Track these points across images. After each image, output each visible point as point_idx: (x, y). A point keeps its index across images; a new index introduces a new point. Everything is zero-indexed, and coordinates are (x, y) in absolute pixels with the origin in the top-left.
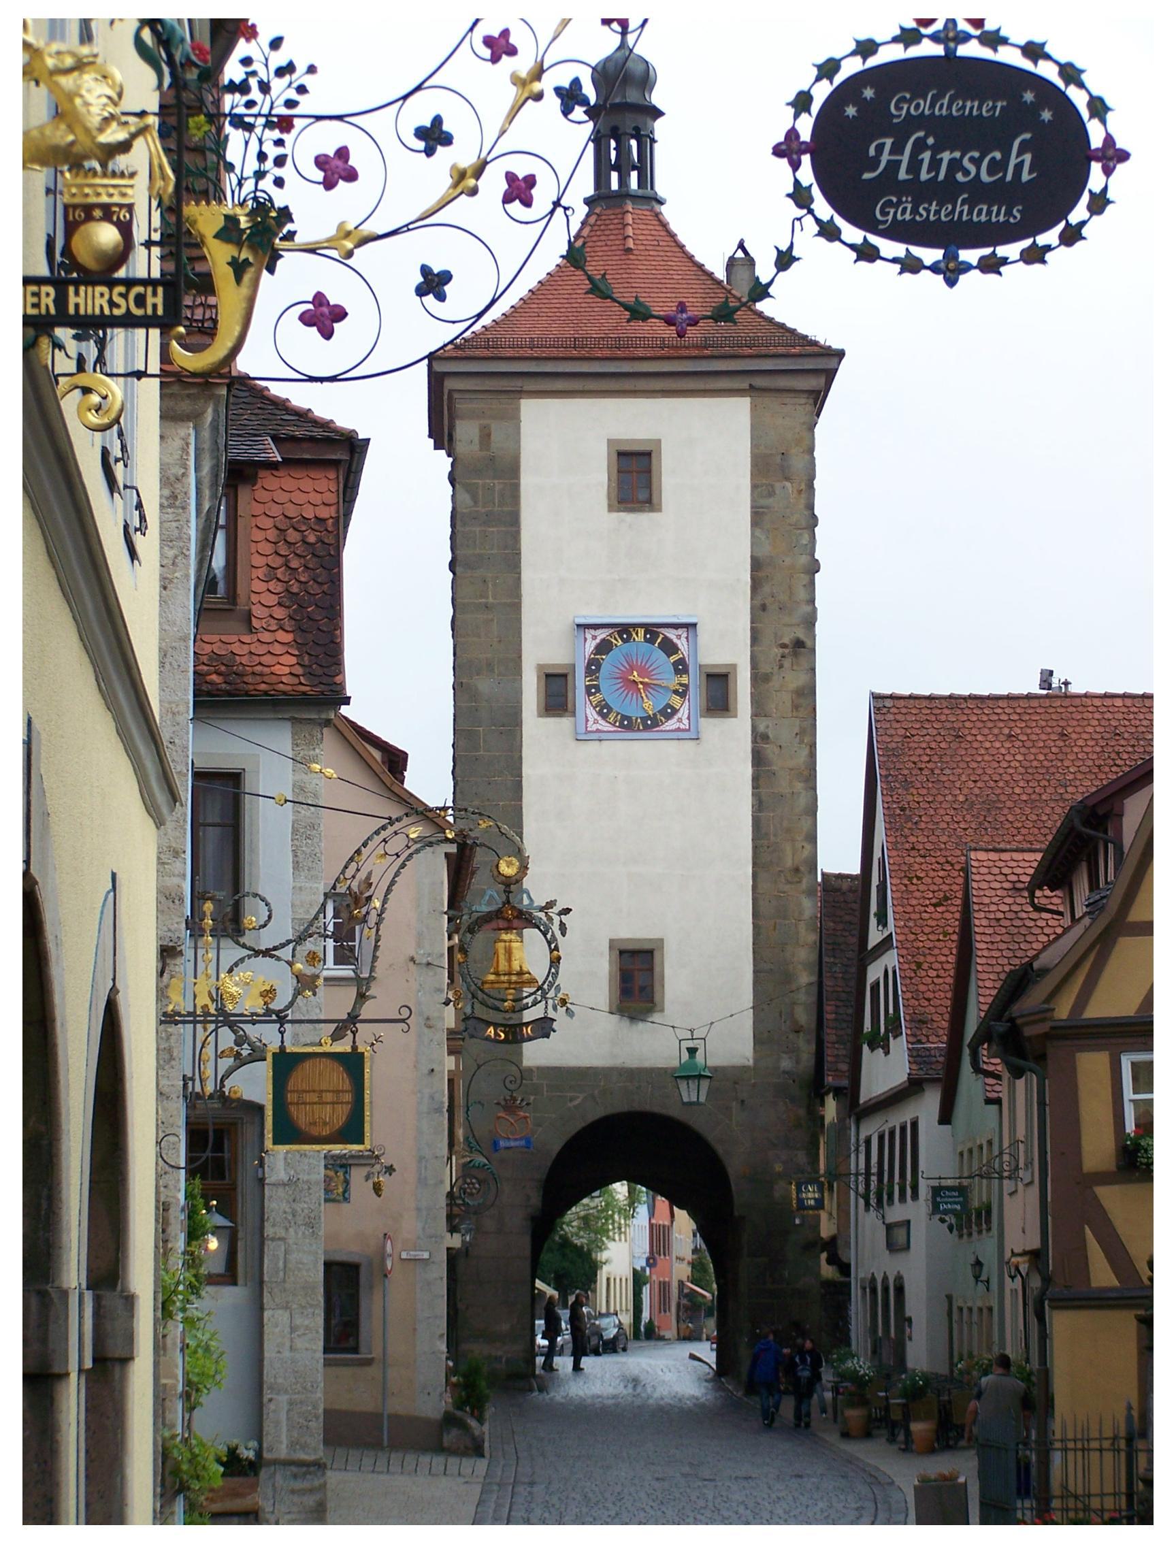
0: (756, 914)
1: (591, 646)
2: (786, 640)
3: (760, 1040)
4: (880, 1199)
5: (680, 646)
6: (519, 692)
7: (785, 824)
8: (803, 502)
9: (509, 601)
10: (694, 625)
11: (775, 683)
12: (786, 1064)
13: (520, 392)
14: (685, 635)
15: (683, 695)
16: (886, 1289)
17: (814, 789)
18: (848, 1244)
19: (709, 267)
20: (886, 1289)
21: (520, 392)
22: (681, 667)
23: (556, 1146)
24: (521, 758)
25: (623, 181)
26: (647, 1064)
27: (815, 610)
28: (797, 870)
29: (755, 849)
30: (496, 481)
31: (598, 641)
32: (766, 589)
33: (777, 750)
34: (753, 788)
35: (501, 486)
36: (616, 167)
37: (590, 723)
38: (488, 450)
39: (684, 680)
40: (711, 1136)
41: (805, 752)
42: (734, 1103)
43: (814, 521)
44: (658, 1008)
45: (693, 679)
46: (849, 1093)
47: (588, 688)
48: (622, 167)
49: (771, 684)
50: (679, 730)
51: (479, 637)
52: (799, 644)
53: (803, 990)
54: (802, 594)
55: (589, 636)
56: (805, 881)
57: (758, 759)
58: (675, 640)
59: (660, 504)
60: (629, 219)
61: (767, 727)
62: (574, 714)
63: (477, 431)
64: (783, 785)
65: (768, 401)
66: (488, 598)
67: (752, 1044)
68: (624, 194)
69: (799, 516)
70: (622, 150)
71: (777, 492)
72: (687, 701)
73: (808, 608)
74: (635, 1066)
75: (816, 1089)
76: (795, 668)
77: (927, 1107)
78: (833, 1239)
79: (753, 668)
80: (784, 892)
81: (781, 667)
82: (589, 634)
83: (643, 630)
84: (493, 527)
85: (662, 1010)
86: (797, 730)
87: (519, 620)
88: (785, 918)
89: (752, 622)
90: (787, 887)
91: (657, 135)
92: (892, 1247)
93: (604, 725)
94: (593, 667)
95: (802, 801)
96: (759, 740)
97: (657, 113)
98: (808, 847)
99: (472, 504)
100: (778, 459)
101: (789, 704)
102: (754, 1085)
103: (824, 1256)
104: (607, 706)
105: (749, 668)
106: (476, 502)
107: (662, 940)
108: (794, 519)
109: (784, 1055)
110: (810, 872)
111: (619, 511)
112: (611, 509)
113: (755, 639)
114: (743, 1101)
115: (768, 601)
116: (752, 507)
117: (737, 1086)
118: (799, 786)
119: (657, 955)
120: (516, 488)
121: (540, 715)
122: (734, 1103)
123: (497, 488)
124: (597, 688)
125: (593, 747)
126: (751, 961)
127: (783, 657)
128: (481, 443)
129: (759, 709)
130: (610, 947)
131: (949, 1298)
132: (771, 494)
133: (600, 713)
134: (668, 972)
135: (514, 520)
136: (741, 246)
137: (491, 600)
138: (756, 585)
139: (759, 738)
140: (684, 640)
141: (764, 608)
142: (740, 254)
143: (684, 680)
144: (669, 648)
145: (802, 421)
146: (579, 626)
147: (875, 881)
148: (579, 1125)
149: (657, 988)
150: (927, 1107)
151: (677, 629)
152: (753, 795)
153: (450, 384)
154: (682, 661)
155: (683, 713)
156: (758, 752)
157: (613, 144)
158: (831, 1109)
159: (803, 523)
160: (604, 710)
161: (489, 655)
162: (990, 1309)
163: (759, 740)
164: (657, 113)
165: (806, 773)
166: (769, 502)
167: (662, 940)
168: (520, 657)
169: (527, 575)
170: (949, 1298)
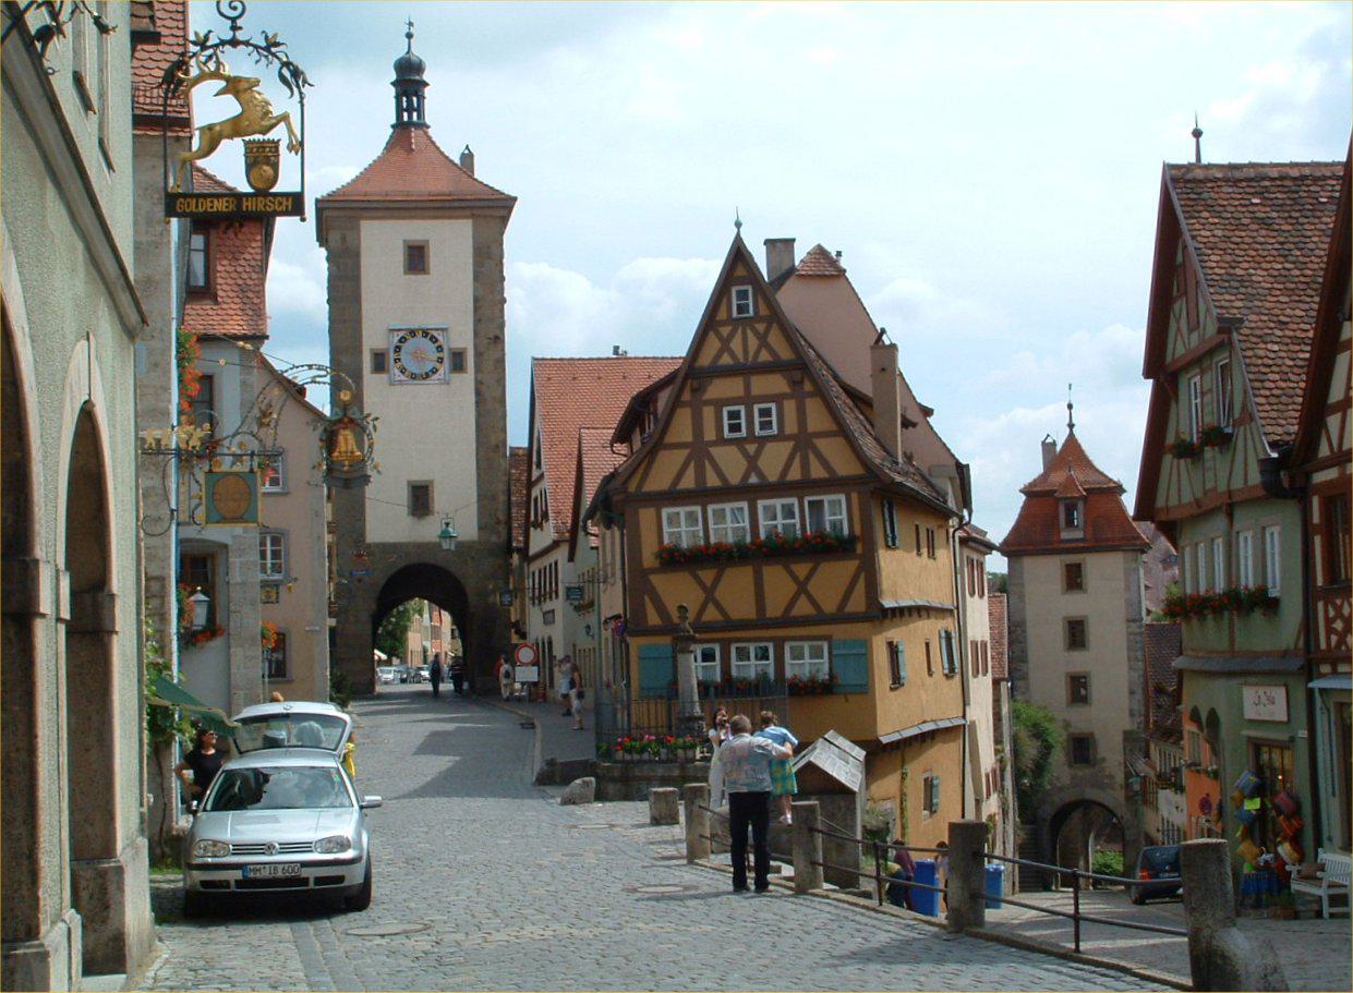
1: (396, 339)
2: (491, 336)
3: (480, 528)
4: (540, 598)
6: (361, 362)
10: (446, 329)
12: (494, 539)
16: (543, 644)
17: (505, 406)
18: (524, 623)
19: (452, 157)
20: (543, 644)
22: (440, 349)
23: (383, 582)
25: (410, 116)
26: (426, 540)
28: (497, 446)
29: (478, 436)
36: (406, 110)
39: (441, 355)
41: (500, 388)
43: (503, 279)
45: (445, 355)
46: (524, 551)
48: (410, 110)
57: (478, 393)
60: (413, 134)
68: (410, 123)
70: (410, 102)
75: (508, 550)
77: (561, 554)
78: (517, 622)
82: (395, 333)
91: (426, 95)
92: (546, 623)
93: (403, 378)
94: (398, 349)
97: (426, 84)
103: (513, 630)
112: (405, 273)
113: (476, 334)
119: (430, 488)
125: (398, 388)
127: (489, 344)
129: (478, 369)
131: (574, 646)
134: (435, 495)
136: (467, 147)
138: (476, 309)
139: (478, 383)
141: (480, 320)
142: (467, 152)
143: (441, 355)
144: (434, 340)
147: (535, 448)
148: (395, 570)
149: (430, 500)
150: (561, 554)
153: (326, 213)
154: (440, 346)
155: (441, 371)
157: (405, 99)
158: (516, 558)
160: (403, 370)
162: (594, 649)
164: (426, 84)
166: (482, 269)
169: (365, 306)
170: (574, 646)
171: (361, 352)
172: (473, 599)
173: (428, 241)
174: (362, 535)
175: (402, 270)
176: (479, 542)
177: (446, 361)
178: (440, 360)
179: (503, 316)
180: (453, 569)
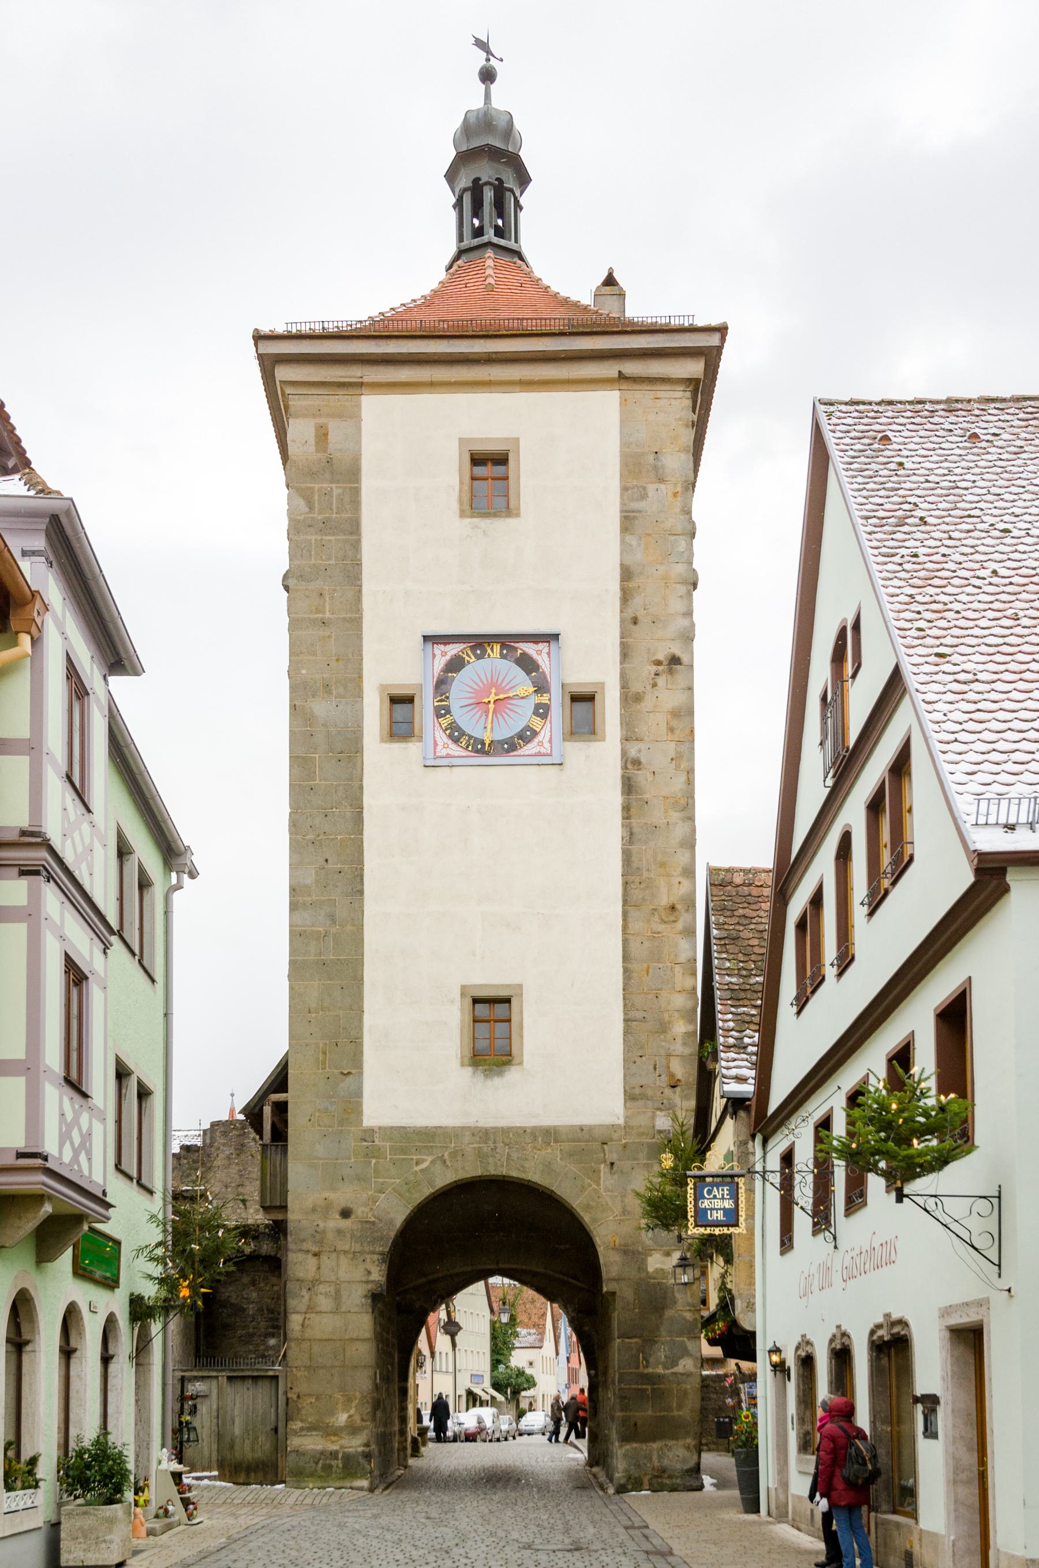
0: (626, 958)
1: (440, 663)
2: (661, 657)
3: (630, 1097)
5: (540, 662)
7: (660, 858)
8: (678, 503)
9: (349, 615)
10: (556, 637)
11: (648, 704)
12: (663, 1122)
13: (361, 385)
14: (546, 650)
15: (544, 716)
17: (691, 818)
21: (361, 385)
24: (361, 788)
27: (693, 625)
29: (626, 884)
30: (334, 486)
31: (448, 657)
32: (637, 601)
33: (650, 777)
34: (624, 818)
35: (340, 491)
37: (439, 748)
38: (325, 451)
39: (544, 699)
40: (576, 1202)
41: (683, 778)
42: (603, 1166)
44: (516, 1061)
45: (556, 699)
47: (437, 709)
49: (643, 704)
50: (539, 754)
51: (315, 654)
52: (675, 660)
53: (679, 1041)
54: (676, 605)
55: (437, 652)
56: (681, 919)
57: (629, 786)
58: (535, 656)
59: (519, 509)
61: (640, 751)
62: (420, 739)
63: (312, 430)
64: (657, 815)
65: (643, 395)
66: (324, 612)
67: (623, 1101)
69: (676, 522)
71: (650, 495)
72: (548, 723)
73: (686, 622)
74: (491, 1125)
76: (669, 686)
79: (623, 687)
80: (659, 933)
81: (655, 685)
82: (439, 649)
83: (499, 646)
84: (330, 534)
85: (521, 1063)
86: (672, 754)
87: (360, 637)
88: (659, 961)
89: (622, 637)
90: (661, 927)
93: (455, 749)
94: (441, 685)
95: (680, 831)
96: (629, 766)
98: (686, 883)
99: (307, 510)
100: (651, 458)
101: (663, 727)
102: (625, 1146)
104: (459, 729)
105: (618, 687)
106: (311, 508)
107: (520, 986)
108: (668, 525)
109: (658, 1113)
110: (687, 910)
111: (472, 517)
112: (462, 514)
113: (625, 653)
114: (612, 1164)
115: (641, 614)
116: (622, 511)
117: (605, 1147)
118: (675, 816)
120: (356, 492)
121: (382, 741)
122: (603, 1166)
123: (336, 492)
124: (448, 712)
126: (622, 1008)
127: (657, 674)
128: (317, 443)
130: (461, 994)
132: (644, 496)
133: (450, 736)
135: (354, 528)
137: (328, 615)
138: (626, 596)
139: (631, 764)
140: (545, 656)
141: (635, 621)
143: (544, 699)
144: (527, 664)
145: (678, 416)
146: (426, 638)
148: (427, 1191)
151: (536, 643)
152: (623, 826)
155: (544, 736)
156: (629, 779)
159: (679, 528)
160: (455, 733)
161: (325, 676)
163: (629, 766)
165: (683, 802)
167: (520, 986)
168: (361, 677)
171: (359, 694)
172: (610, 1262)
173: (517, 440)
174: (353, 1105)
175: (455, 506)
176: (627, 1127)
177: (556, 713)
178: (542, 711)
179: (689, 614)
180: (565, 1190)
